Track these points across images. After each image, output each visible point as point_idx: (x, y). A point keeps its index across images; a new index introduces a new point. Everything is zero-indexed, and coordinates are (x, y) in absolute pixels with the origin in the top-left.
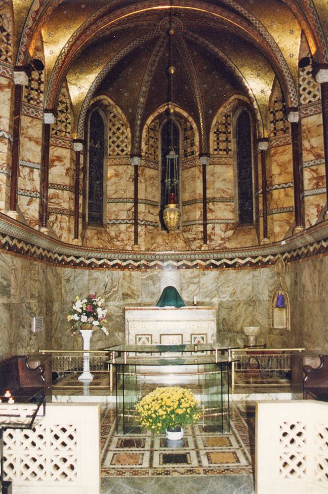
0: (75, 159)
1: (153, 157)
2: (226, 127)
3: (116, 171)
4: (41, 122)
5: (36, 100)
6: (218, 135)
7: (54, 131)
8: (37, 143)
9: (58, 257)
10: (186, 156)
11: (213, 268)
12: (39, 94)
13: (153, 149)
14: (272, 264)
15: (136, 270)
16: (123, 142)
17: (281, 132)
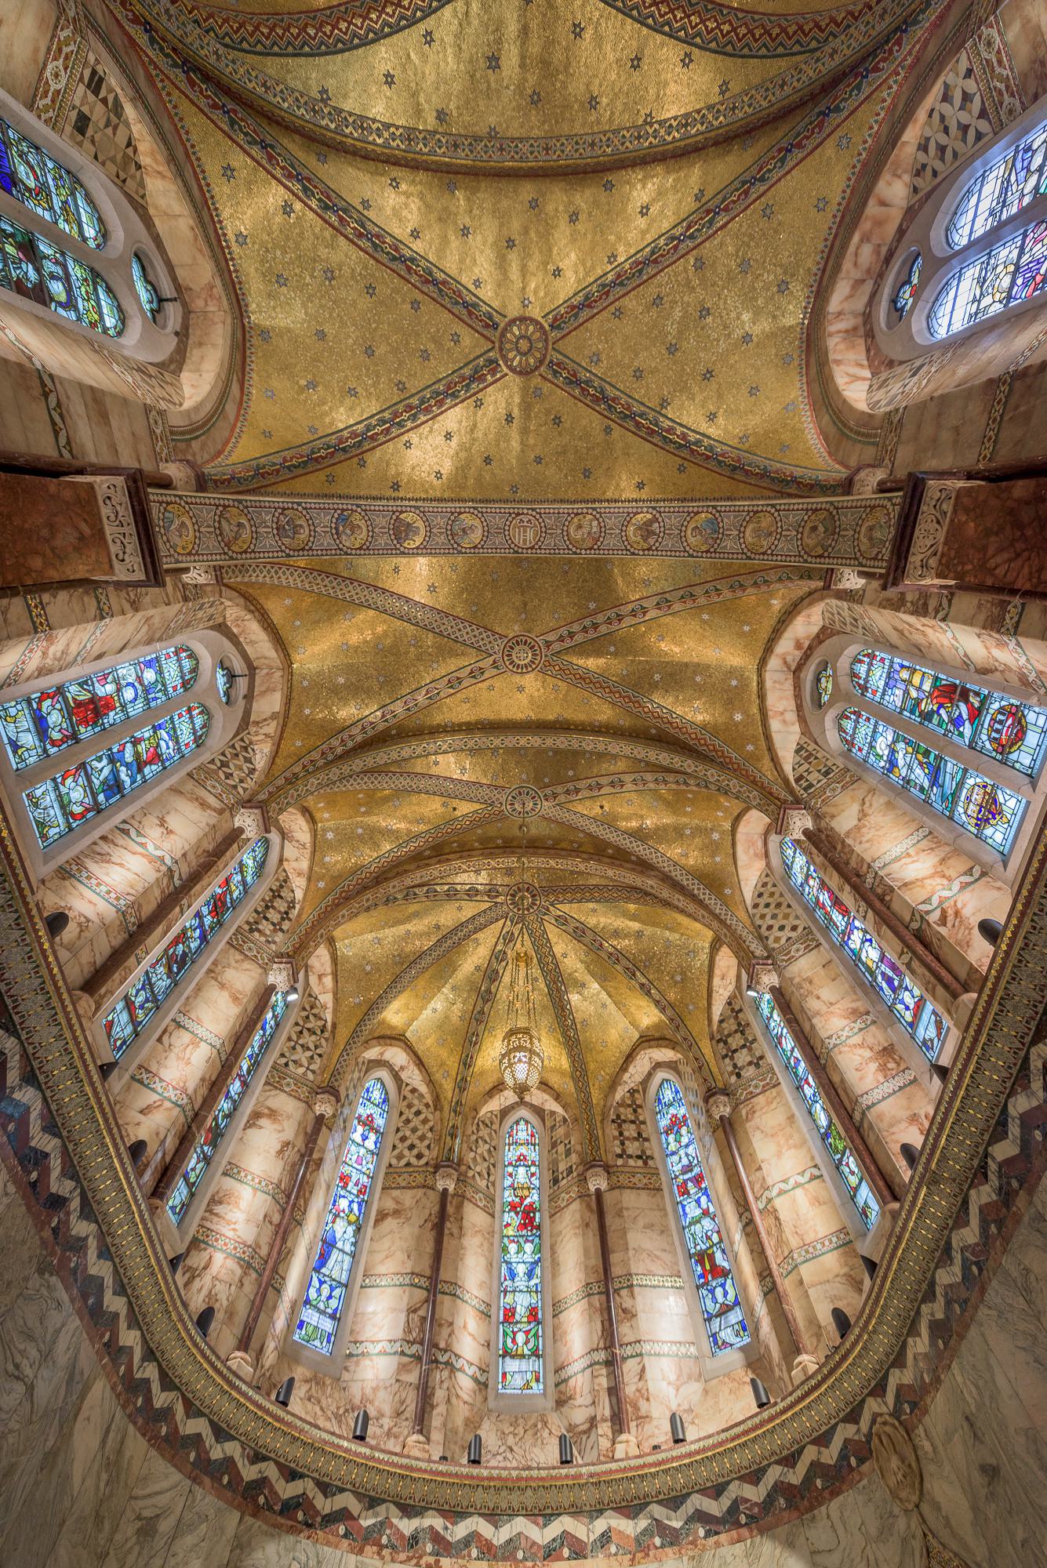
0: (309, 1130)
1: (484, 1183)
2: (635, 1111)
3: (398, 1203)
4: (260, 971)
5: (265, 935)
6: (620, 1126)
7: (284, 1060)
8: (235, 999)
9: (155, 1387)
10: (556, 1181)
11: (663, 1546)
12: (275, 931)
13: (486, 1165)
14: (861, 1461)
15: (403, 1556)
16: (422, 1138)
17: (752, 1068)
